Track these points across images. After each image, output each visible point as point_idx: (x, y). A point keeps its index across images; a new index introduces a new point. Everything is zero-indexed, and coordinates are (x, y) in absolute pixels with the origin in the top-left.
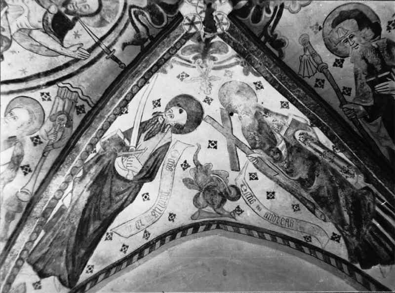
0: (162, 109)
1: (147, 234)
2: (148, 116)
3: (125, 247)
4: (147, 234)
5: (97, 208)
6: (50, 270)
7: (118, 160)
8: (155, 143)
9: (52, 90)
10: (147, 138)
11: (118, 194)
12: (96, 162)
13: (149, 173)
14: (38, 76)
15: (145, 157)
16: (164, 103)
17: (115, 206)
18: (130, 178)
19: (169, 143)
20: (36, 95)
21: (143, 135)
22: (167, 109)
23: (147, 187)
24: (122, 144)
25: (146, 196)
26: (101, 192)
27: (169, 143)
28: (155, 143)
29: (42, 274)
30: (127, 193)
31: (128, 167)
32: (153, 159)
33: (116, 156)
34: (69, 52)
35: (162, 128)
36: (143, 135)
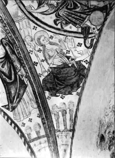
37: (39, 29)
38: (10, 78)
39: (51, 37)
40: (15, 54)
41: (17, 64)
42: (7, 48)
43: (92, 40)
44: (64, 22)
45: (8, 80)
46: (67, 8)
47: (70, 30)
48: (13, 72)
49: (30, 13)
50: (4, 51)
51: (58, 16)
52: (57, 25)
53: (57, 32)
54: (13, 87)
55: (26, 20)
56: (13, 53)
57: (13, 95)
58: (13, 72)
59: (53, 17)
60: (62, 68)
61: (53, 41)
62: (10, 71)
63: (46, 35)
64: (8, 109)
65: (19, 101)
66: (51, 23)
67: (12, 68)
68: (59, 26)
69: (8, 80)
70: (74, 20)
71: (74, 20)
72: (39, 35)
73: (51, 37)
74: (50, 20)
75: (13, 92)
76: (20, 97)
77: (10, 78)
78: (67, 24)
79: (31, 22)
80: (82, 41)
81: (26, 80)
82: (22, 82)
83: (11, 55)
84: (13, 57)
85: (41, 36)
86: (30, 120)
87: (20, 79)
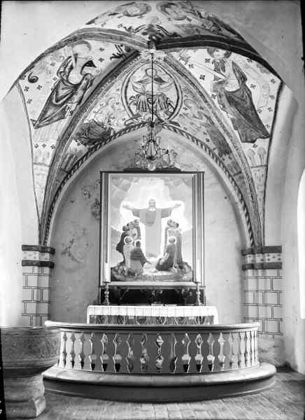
0: (212, 59)
1: (272, 97)
2: (213, 67)
3: (269, 109)
4: (272, 97)
5: (243, 107)
6: (254, 139)
7: (226, 89)
8: (229, 68)
9: (184, 94)
10: (224, 71)
11: (243, 97)
12: (220, 97)
13: (243, 79)
14: (178, 94)
15: (233, 76)
16: (208, 57)
17: (248, 100)
18: (238, 88)
19: (233, 63)
20: (184, 98)
21: (221, 72)
22: (213, 57)
23: (248, 84)
24: (220, 83)
25: (253, 86)
26: (236, 102)
27: (233, 63)
28: (229, 68)
29: (253, 142)
30: (245, 93)
31: (233, 85)
32: (237, 74)
33: (224, 88)
34: (171, 83)
35: (223, 62)
36: (221, 72)
37: (119, 92)
38: (57, 101)
39: (118, 104)
40: (84, 93)
41: (76, 98)
42: (85, 82)
43: (132, 123)
44: (135, 102)
45: (54, 101)
46: (148, 99)
47: (132, 109)
48: (65, 99)
49: (129, 81)
50: (79, 82)
51: (138, 96)
52: (130, 99)
53: (125, 104)
54: (53, 109)
55: (122, 82)
56: (85, 90)
57: (47, 116)
58: (65, 99)
59: (135, 94)
60: (99, 125)
61: (117, 107)
62: (62, 98)
63: (117, 99)
64: (34, 125)
65: (47, 124)
66: (129, 96)
67: (67, 97)
68: (129, 102)
69: (54, 101)
70: (141, 106)
71: (141, 106)
72: (114, 95)
73: (118, 104)
74: (131, 93)
75: (49, 113)
76: (50, 121)
77: (57, 101)
78: (135, 104)
79: (121, 85)
80: (127, 118)
81: (68, 113)
82: (64, 112)
83: (79, 89)
84: (80, 92)
85: (114, 98)
86: (44, 146)
87: (64, 109)
